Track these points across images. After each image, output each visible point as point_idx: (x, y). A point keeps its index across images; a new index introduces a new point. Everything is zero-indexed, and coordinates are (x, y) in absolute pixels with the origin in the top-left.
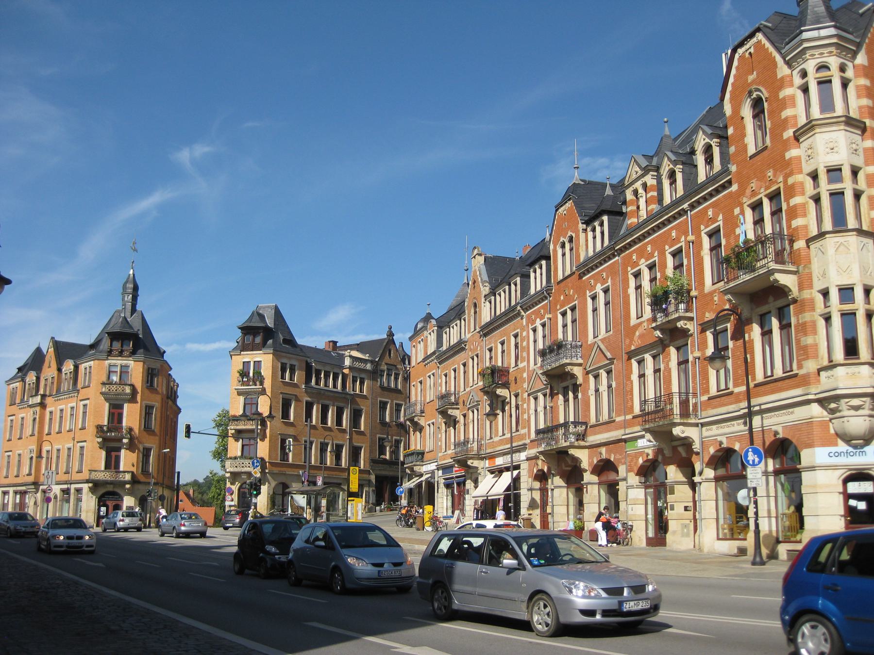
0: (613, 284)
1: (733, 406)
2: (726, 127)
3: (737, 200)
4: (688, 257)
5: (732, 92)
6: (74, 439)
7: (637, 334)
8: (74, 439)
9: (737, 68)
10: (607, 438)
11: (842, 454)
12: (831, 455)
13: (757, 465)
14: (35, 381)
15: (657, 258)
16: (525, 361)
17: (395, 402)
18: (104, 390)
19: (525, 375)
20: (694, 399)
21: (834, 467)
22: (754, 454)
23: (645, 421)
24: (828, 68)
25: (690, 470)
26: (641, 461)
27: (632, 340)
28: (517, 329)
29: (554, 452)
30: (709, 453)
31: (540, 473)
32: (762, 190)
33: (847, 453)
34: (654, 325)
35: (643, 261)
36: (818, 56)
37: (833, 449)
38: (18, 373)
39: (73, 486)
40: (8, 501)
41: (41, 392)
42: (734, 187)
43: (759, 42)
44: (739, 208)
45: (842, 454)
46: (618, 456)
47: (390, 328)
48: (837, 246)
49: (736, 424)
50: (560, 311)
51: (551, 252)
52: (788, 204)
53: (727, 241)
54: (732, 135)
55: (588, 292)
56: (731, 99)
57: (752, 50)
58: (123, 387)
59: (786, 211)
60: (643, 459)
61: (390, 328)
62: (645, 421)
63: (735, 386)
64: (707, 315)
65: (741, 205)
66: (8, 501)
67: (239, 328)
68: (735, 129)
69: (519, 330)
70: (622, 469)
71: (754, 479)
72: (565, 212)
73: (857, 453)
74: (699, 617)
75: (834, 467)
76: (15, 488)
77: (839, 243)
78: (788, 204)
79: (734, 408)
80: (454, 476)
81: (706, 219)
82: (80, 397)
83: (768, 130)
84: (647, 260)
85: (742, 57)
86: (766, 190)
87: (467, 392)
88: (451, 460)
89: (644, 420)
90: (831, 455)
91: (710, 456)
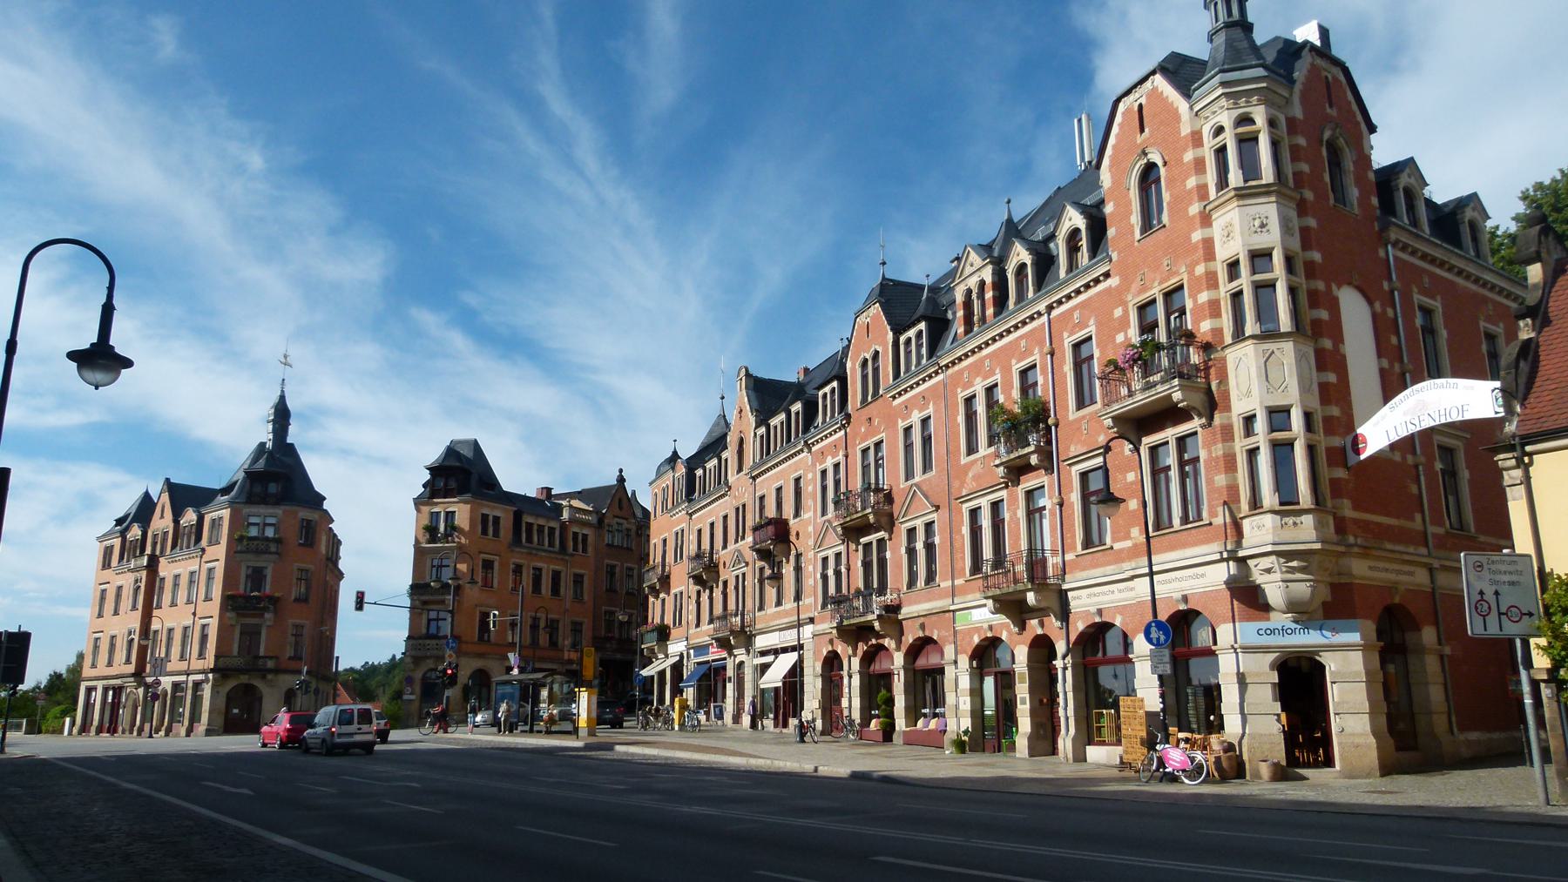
0: (935, 411)
1: (1112, 567)
2: (1102, 202)
3: (1117, 296)
4: (1044, 372)
5: (1112, 158)
6: (194, 614)
7: (970, 475)
8: (194, 614)
9: (1121, 126)
10: (929, 610)
11: (1276, 631)
12: (1261, 632)
13: (1162, 644)
14: (139, 537)
15: (999, 375)
16: (810, 511)
17: (625, 565)
18: (239, 548)
19: (811, 529)
20: (1055, 558)
21: (1265, 649)
22: (1159, 630)
23: (987, 587)
24: (1252, 122)
25: (1045, 652)
26: (976, 640)
27: (963, 483)
28: (800, 469)
29: (854, 628)
30: (1077, 629)
31: (832, 655)
32: (1156, 284)
33: (1283, 630)
34: (997, 462)
35: (979, 380)
36: (1244, 105)
37: (1263, 625)
38: (116, 526)
39: (192, 678)
40: (95, 700)
41: (148, 551)
42: (1113, 282)
43: (1155, 89)
44: (1120, 308)
45: (1276, 631)
46: (944, 633)
47: (621, 471)
48: (1267, 355)
49: (1116, 590)
50: (860, 446)
51: (848, 371)
52: (1195, 301)
53: (1102, 352)
54: (1112, 213)
55: (900, 421)
56: (1111, 166)
57: (1143, 101)
58: (267, 545)
59: (1192, 310)
60: (979, 636)
61: (621, 471)
62: (987, 587)
63: (1114, 540)
64: (1072, 448)
65: (1124, 304)
66: (95, 700)
67: (428, 469)
68: (1117, 206)
69: (802, 472)
70: (949, 651)
71: (1160, 663)
72: (868, 319)
73: (1297, 631)
74: (1074, 854)
75: (1265, 649)
76: (105, 682)
77: (1270, 352)
78: (1195, 301)
79: (1114, 570)
80: (710, 659)
81: (1070, 325)
82: (205, 558)
83: (1165, 204)
84: (985, 378)
85: (1128, 111)
86: (1160, 284)
87: (730, 552)
88: (708, 638)
89: (986, 585)
90: (1261, 632)
91: (1078, 633)
